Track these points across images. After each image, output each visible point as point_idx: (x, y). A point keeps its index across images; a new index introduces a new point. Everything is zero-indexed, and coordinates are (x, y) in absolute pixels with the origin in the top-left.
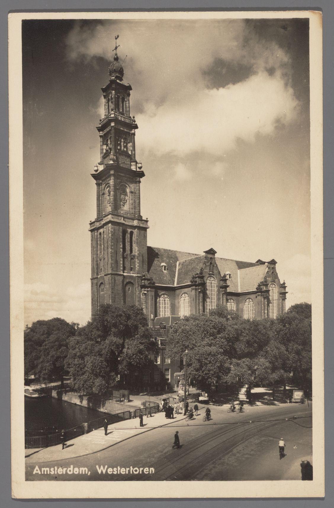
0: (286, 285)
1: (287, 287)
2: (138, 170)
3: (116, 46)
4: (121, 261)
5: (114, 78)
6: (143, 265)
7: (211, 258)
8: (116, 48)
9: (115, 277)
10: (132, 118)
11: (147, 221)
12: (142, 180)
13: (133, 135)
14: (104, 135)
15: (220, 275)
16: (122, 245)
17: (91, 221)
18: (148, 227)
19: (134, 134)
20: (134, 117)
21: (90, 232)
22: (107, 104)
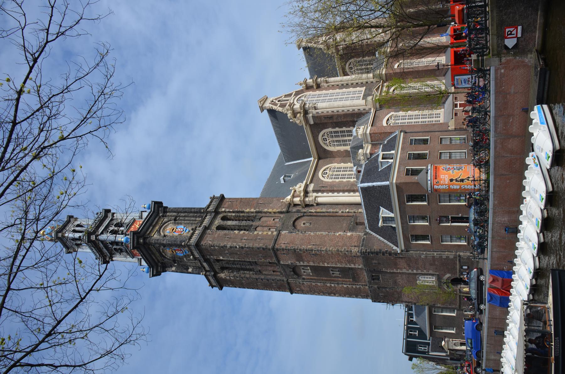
13: (115, 215)
19: (114, 213)
21: (224, 288)
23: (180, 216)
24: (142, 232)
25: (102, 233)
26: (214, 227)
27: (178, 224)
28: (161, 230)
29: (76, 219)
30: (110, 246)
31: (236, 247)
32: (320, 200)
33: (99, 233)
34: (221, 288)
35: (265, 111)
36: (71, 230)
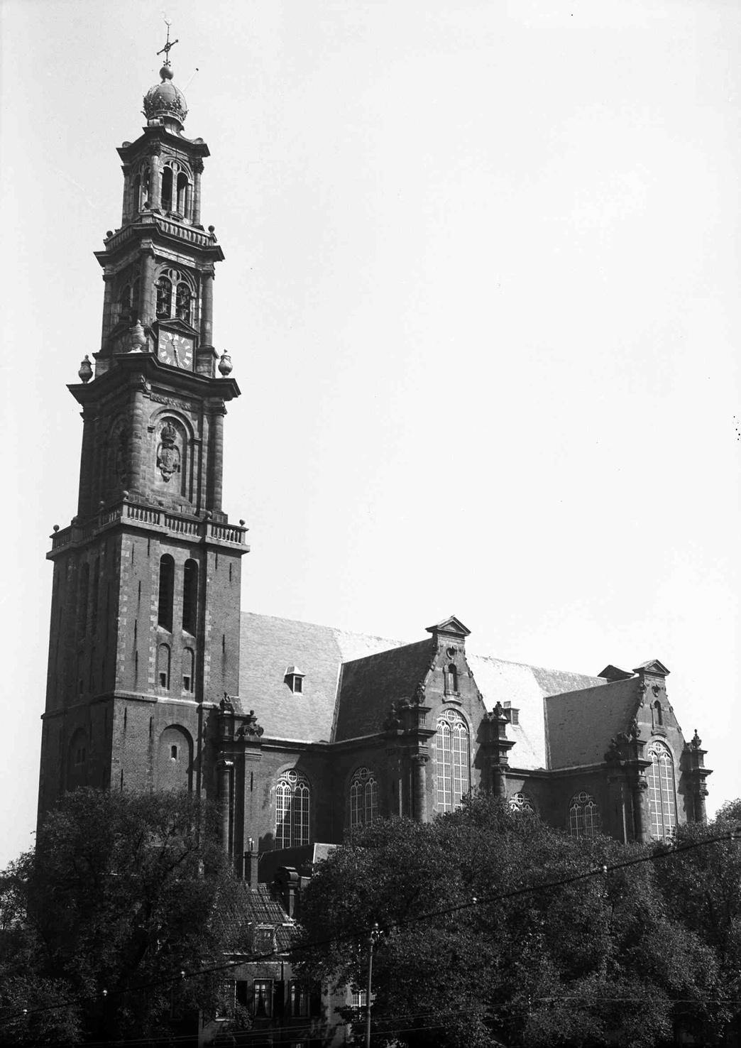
0: (702, 747)
1: (706, 752)
2: (219, 375)
3: (168, 43)
4: (151, 655)
5: (158, 121)
6: (224, 670)
7: (452, 651)
8: (168, 47)
9: (129, 708)
10: (207, 232)
11: (240, 530)
12: (228, 405)
14: (118, 274)
15: (484, 708)
16: (157, 603)
17: (56, 528)
18: (244, 548)
19: (211, 274)
20: (211, 229)
21: (52, 563)
22: (132, 191)
23: (200, 451)
24: (158, 373)
25: (159, 259)
26: (165, 549)
27: (185, 450)
28: (168, 415)
29: (198, 168)
30: (133, 279)
31: (117, 616)
32: (227, 777)
33: (157, 253)
34: (49, 557)
35: (430, 635)
36: (170, 167)
